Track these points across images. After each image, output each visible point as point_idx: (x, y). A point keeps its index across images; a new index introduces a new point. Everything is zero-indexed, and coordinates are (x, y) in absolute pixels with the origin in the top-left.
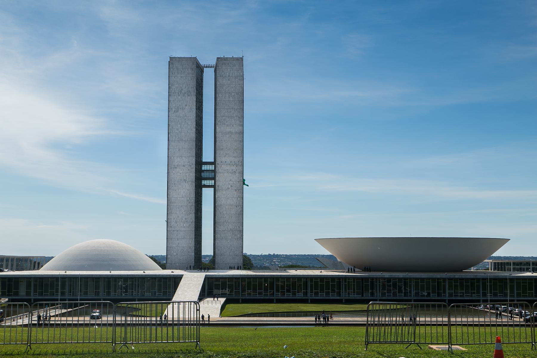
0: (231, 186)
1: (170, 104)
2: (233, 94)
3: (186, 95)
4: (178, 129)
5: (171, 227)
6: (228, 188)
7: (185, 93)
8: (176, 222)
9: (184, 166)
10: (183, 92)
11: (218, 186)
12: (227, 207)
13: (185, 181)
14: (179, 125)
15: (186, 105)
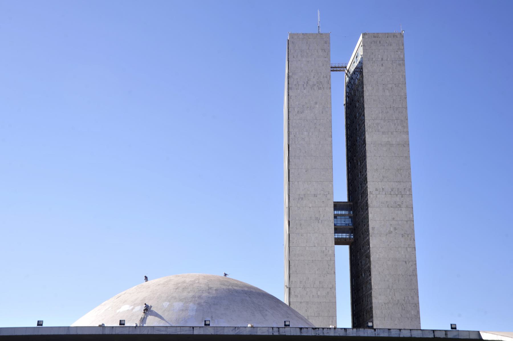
0: (395, 229)
1: (291, 100)
2: (390, 86)
3: (315, 88)
4: (303, 139)
5: (296, 296)
6: (390, 232)
7: (314, 85)
8: (304, 288)
9: (315, 195)
10: (311, 83)
11: (373, 228)
12: (389, 263)
13: (317, 219)
14: (306, 133)
15: (316, 103)
